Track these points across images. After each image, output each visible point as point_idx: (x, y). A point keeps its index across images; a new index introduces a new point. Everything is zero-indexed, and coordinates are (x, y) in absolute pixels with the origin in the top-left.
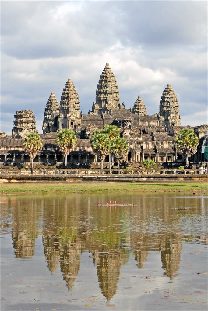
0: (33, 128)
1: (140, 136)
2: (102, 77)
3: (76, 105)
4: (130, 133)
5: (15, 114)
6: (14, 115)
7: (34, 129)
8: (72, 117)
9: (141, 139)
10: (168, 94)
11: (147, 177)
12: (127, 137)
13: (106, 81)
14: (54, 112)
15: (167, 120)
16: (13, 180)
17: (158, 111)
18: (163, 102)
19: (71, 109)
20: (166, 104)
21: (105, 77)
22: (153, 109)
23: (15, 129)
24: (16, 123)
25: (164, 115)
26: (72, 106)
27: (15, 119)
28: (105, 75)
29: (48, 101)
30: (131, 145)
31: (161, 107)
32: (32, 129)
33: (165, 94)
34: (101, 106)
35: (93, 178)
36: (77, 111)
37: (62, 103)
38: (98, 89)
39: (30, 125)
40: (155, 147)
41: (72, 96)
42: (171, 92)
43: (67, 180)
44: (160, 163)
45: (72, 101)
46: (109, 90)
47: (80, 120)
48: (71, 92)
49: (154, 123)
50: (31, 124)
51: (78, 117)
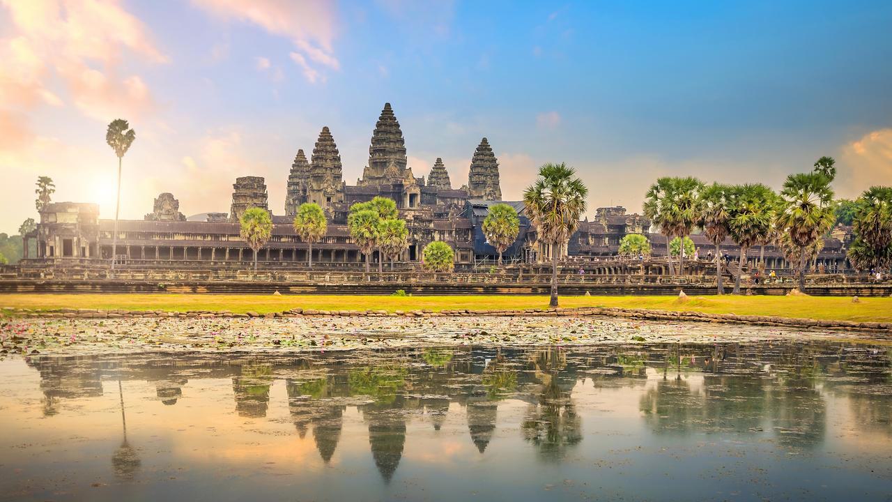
1: (430, 221)
2: (379, 125)
3: (336, 171)
4: (413, 216)
5: (235, 183)
6: (234, 185)
7: (265, 207)
9: (432, 226)
10: (482, 154)
11: (424, 287)
13: (386, 132)
14: (303, 180)
16: (200, 289)
17: (466, 182)
19: (329, 176)
21: (384, 124)
22: (459, 177)
24: (235, 196)
26: (328, 172)
27: (234, 191)
29: (294, 163)
30: (415, 236)
32: (263, 207)
35: (335, 286)
36: (337, 179)
37: (316, 167)
38: (372, 145)
41: (330, 156)
43: (292, 289)
44: (462, 264)
45: (329, 164)
47: (343, 195)
48: (329, 148)
49: (460, 202)
50: (260, 199)
51: (339, 189)
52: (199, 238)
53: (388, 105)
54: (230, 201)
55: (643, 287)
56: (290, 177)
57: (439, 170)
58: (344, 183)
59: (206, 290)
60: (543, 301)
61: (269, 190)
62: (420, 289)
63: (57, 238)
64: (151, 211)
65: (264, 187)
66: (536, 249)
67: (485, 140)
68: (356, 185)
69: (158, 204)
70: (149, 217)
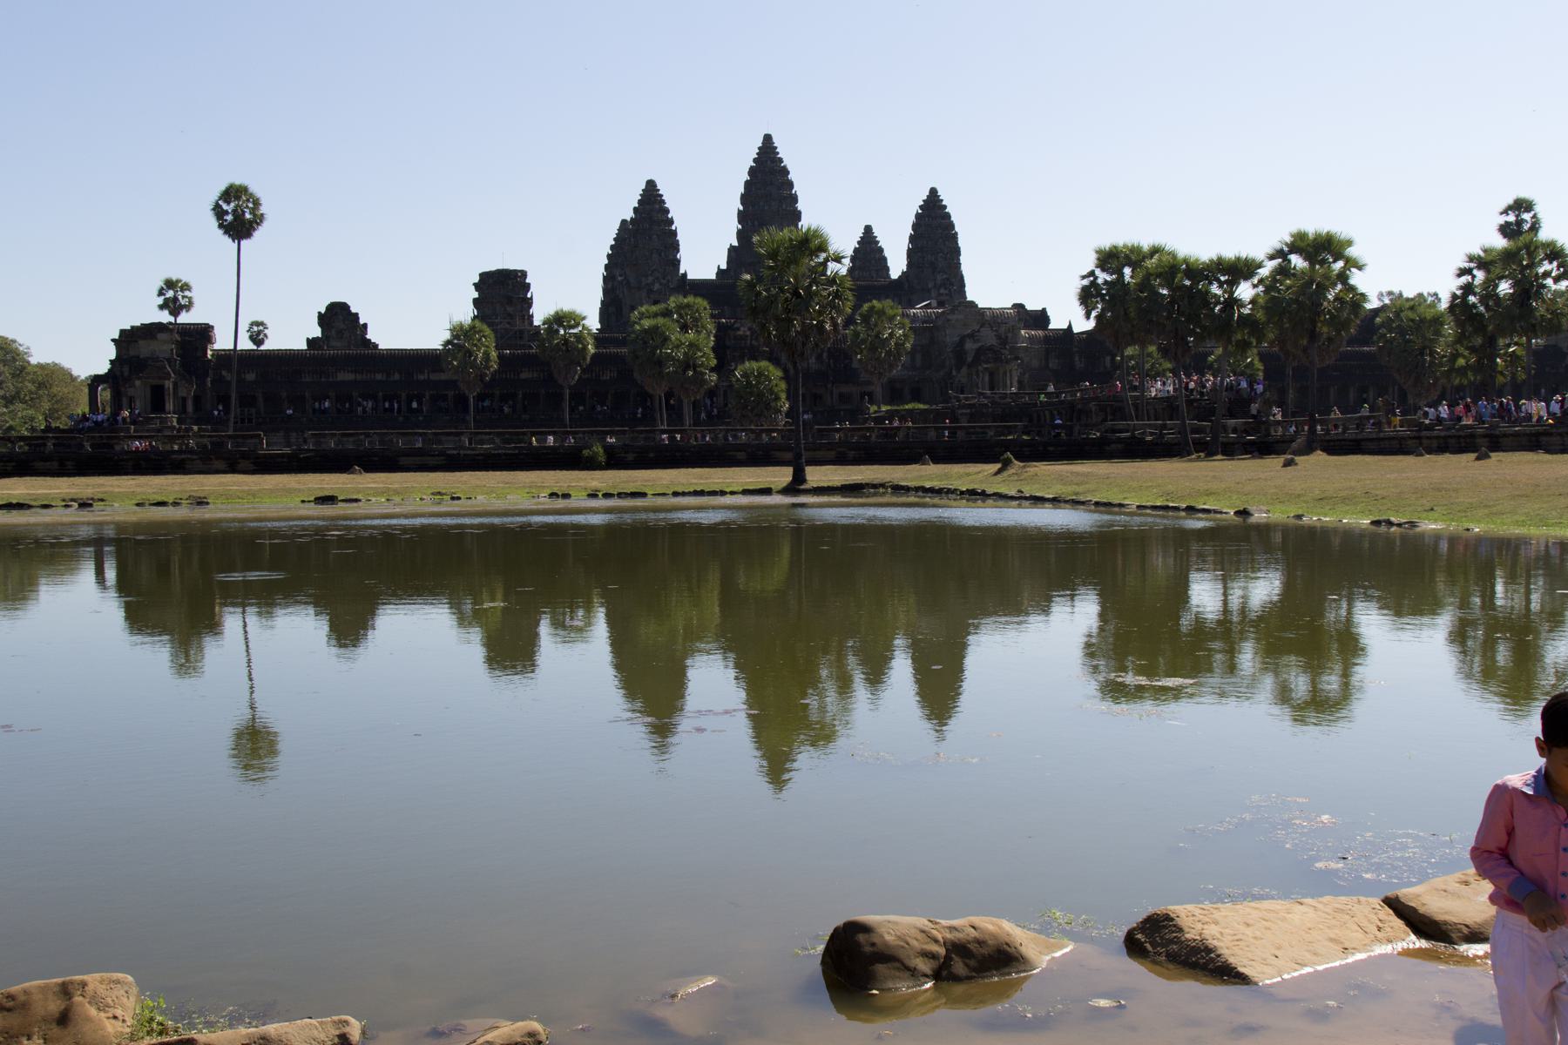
2: (752, 171)
5: (477, 280)
8: (657, 287)
12: (743, 338)
16: (243, 464)
27: (476, 295)
43: (404, 461)
53: (768, 139)
57: (869, 249)
58: (685, 275)
59: (252, 467)
60: (783, 475)
61: (536, 292)
62: (630, 457)
63: (138, 383)
66: (964, 380)
67: (933, 192)
68: (713, 277)
69: (323, 319)
70: (310, 342)
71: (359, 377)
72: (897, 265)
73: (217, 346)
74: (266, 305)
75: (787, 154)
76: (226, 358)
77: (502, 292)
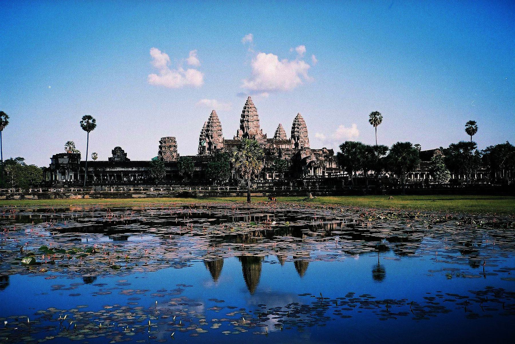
0: (176, 151)
10: (298, 121)
15: (297, 145)
18: (293, 128)
19: (215, 135)
20: (296, 129)
23: (160, 153)
24: (160, 147)
25: (295, 140)
27: (160, 144)
28: (247, 106)
31: (293, 132)
33: (296, 121)
34: (244, 132)
39: (172, 149)
40: (265, 166)
42: (300, 120)
43: (133, 196)
45: (215, 129)
46: (250, 119)
52: (130, 169)
54: (158, 149)
55: (326, 192)
56: (201, 136)
61: (178, 144)
62: (201, 195)
64: (111, 156)
65: (175, 142)
69: (114, 152)
70: (110, 159)
71: (123, 169)
72: (289, 136)
73: (81, 160)
74: (97, 148)
75: (255, 101)
76: (83, 163)
77: (167, 144)
